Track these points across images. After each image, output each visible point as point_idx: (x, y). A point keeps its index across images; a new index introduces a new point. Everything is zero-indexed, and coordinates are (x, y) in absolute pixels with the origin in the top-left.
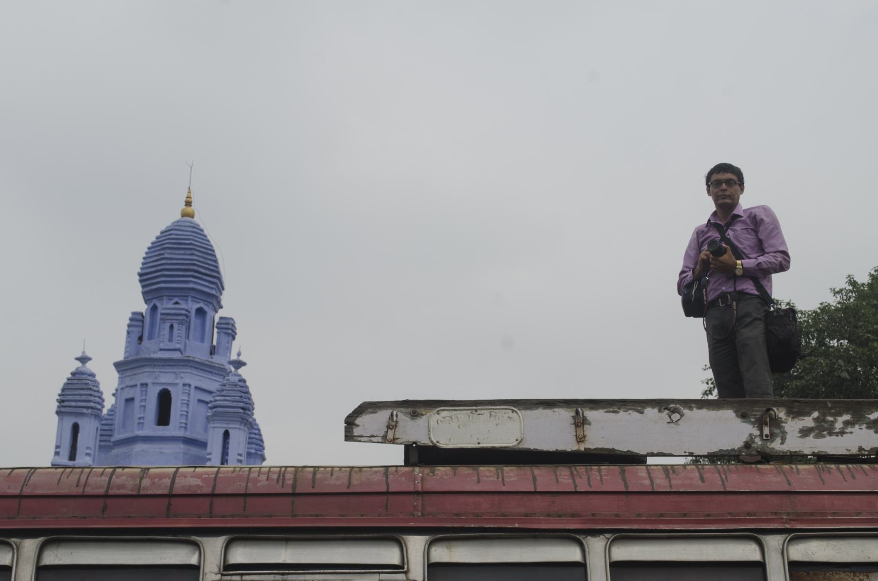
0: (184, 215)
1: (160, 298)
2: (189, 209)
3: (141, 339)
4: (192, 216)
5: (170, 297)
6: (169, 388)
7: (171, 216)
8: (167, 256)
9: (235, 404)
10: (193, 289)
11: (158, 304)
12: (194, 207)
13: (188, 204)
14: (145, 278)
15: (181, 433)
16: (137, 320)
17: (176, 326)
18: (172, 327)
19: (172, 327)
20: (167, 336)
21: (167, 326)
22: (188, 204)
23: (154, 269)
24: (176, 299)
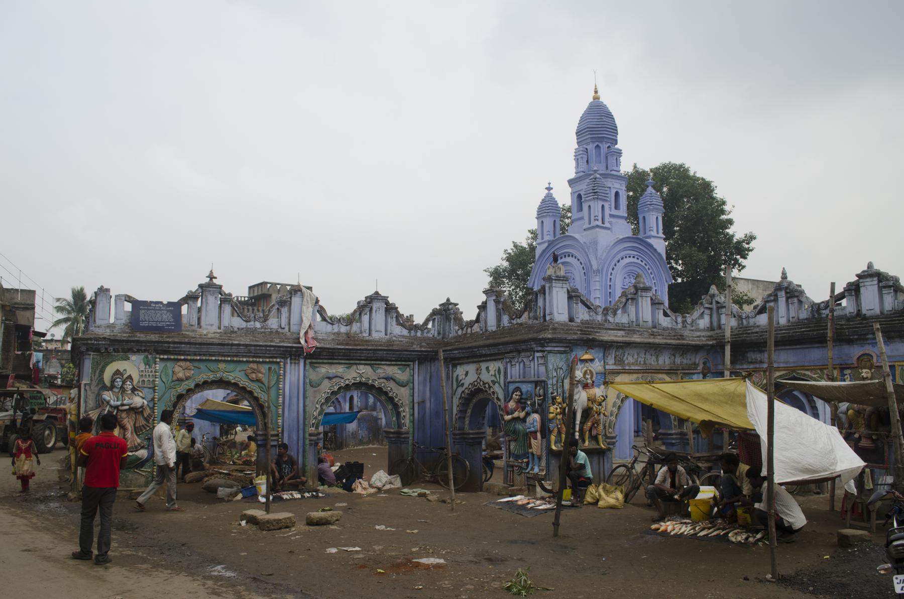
0: (595, 98)
1: (601, 142)
4: (599, 99)
6: (619, 191)
11: (600, 145)
12: (599, 94)
13: (596, 92)
22: (596, 92)
23: (600, 126)
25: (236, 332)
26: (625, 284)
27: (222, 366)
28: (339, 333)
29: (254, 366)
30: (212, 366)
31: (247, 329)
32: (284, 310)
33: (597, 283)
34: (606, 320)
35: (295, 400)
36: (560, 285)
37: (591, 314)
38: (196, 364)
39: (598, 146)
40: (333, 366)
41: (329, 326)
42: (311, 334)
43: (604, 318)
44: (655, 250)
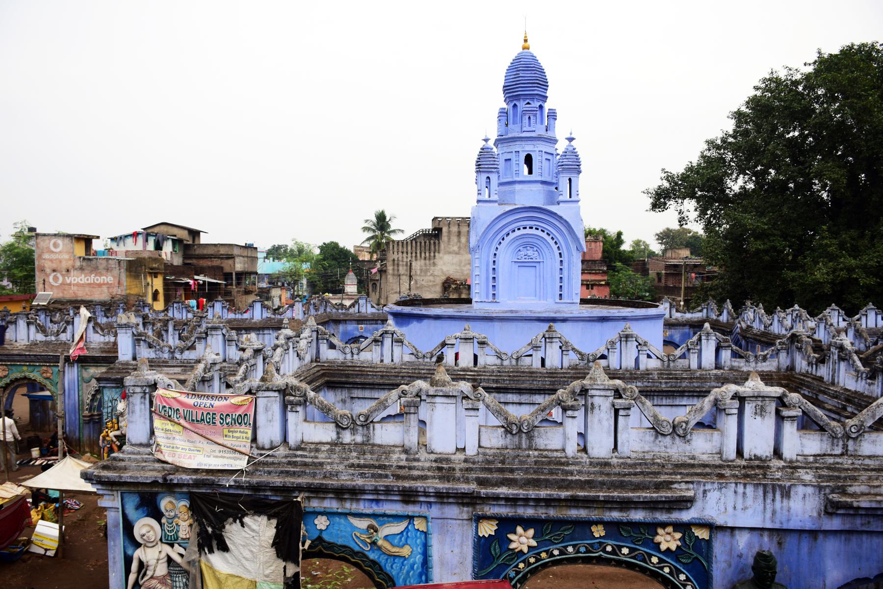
0: (524, 48)
1: (519, 100)
2: (526, 45)
3: (507, 125)
4: (529, 49)
5: (524, 100)
6: (531, 153)
7: (516, 50)
8: (521, 75)
9: (574, 163)
10: (537, 94)
11: (517, 103)
13: (526, 41)
14: (506, 89)
15: (539, 179)
16: (503, 113)
17: (532, 117)
18: (529, 118)
19: (529, 118)
20: (527, 124)
21: (527, 117)
22: (526, 41)
24: (528, 101)
25: (37, 344)
26: (519, 257)
27: (25, 368)
28: (108, 343)
29: (45, 368)
30: (19, 368)
31: (46, 341)
32: (69, 328)
33: (477, 260)
34: (173, 358)
35: (72, 392)
36: (124, 331)
37: (157, 353)
38: (10, 367)
39: (515, 106)
40: (99, 368)
41: (102, 337)
42: (81, 344)
43: (171, 356)
44: (561, 217)
